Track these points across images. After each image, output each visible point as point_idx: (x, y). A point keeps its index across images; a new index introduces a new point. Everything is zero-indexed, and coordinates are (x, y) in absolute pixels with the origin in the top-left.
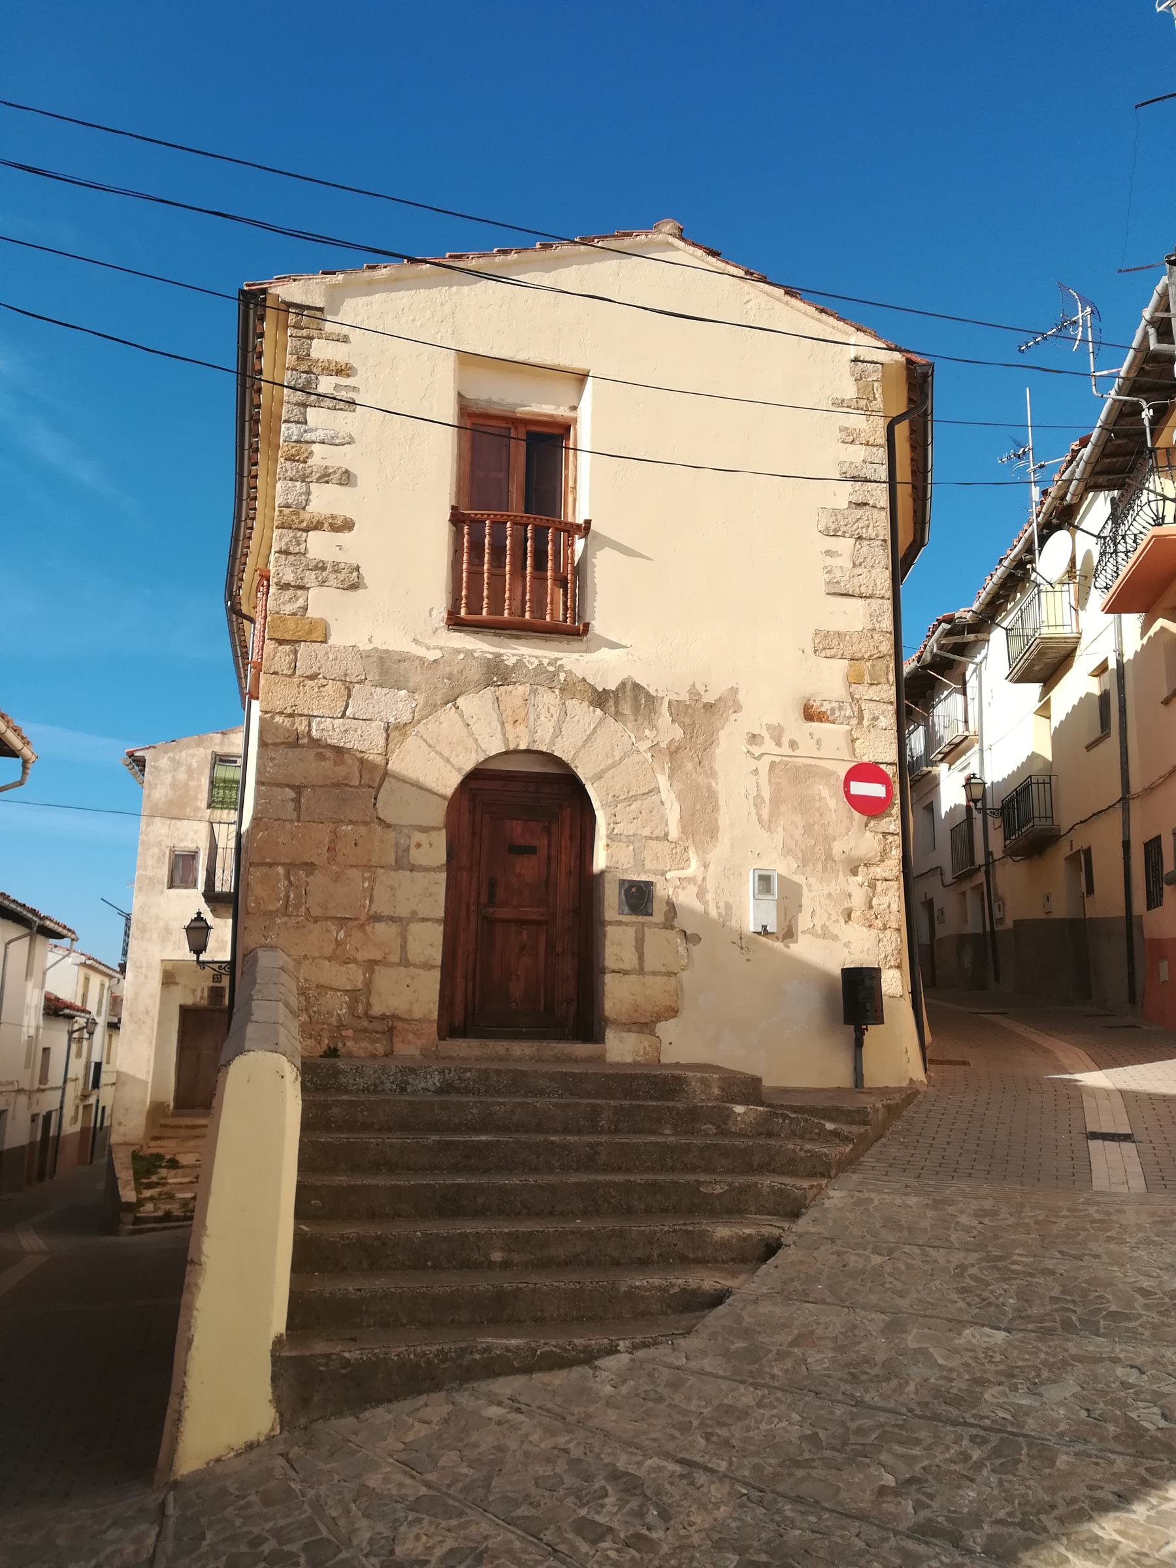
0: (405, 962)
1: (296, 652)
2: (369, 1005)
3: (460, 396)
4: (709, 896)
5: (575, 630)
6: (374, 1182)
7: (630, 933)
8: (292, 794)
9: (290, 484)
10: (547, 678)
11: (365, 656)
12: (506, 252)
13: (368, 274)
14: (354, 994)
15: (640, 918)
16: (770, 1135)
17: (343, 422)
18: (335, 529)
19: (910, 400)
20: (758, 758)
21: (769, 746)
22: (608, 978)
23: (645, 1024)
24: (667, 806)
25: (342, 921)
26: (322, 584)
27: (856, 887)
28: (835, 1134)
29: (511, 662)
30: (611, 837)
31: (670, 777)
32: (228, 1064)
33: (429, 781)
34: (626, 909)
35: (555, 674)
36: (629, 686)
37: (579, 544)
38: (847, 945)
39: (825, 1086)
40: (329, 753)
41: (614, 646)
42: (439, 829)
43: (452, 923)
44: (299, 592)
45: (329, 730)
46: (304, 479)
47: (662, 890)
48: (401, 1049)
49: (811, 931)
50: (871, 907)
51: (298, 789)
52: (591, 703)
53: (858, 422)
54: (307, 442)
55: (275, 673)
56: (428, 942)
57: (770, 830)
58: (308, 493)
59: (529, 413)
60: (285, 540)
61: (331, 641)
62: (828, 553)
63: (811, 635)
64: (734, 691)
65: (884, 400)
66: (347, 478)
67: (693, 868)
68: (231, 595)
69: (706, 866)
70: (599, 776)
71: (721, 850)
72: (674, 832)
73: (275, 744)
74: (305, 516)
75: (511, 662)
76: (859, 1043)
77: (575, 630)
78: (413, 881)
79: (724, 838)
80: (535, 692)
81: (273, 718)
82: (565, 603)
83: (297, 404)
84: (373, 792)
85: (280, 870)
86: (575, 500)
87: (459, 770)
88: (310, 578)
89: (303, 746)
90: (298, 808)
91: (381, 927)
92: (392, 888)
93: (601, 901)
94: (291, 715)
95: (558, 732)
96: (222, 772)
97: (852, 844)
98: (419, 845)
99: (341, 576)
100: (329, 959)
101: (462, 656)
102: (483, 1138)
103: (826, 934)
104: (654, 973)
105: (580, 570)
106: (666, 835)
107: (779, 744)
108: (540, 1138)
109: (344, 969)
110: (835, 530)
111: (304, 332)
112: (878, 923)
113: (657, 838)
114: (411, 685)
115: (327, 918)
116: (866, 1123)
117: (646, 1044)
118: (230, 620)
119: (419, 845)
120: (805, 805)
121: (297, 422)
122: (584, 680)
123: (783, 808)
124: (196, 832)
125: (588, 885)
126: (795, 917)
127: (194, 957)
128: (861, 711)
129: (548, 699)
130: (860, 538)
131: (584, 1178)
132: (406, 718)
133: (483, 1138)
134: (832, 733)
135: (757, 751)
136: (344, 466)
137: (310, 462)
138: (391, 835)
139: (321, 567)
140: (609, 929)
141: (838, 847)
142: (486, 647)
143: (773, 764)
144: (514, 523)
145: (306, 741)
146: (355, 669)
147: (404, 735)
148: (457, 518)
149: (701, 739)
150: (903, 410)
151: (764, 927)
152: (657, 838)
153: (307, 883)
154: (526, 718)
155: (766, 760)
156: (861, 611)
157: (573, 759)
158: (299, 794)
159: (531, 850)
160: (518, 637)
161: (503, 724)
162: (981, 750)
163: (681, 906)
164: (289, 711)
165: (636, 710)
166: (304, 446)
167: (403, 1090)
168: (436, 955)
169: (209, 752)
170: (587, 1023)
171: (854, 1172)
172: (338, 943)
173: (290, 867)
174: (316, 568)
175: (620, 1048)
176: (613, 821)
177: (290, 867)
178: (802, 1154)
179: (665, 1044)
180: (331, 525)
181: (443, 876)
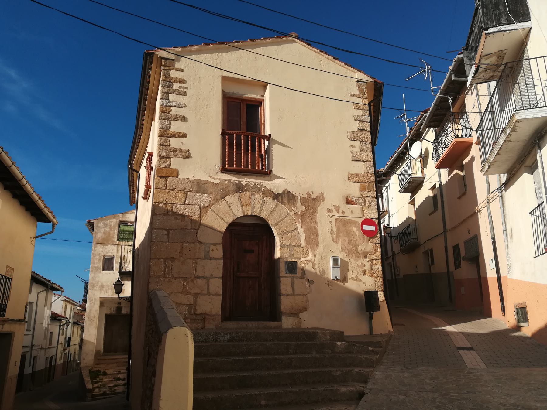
0: (208, 293)
1: (166, 181)
2: (196, 310)
3: (223, 91)
4: (317, 267)
5: (266, 173)
6: (213, 376)
7: (289, 280)
8: (166, 232)
9: (164, 121)
10: (257, 189)
11: (192, 182)
12: (238, 42)
13: (190, 48)
14: (190, 306)
15: (293, 275)
16: (350, 352)
17: (182, 100)
18: (180, 137)
19: (375, 95)
20: (331, 217)
21: (335, 213)
22: (282, 297)
23: (295, 313)
24: (301, 234)
25: (185, 279)
26: (176, 156)
27: (366, 262)
28: (372, 351)
29: (244, 184)
30: (282, 246)
31: (301, 224)
32: (166, 332)
33: (216, 227)
34: (288, 272)
35: (260, 188)
36: (286, 192)
37: (267, 143)
38: (365, 283)
39: (359, 334)
40: (179, 217)
41: (280, 178)
42: (220, 244)
43: (225, 278)
44: (168, 159)
45: (179, 208)
46: (169, 119)
47: (301, 265)
48: (208, 326)
49: (352, 278)
50: (372, 269)
51: (168, 230)
52: (273, 198)
53: (359, 101)
54: (169, 106)
55: (159, 188)
56: (217, 285)
57: (336, 242)
58: (170, 124)
59: (247, 97)
60: (162, 141)
61: (179, 177)
62: (352, 146)
63: (347, 174)
64: (322, 194)
65: (368, 95)
66: (184, 119)
67: (311, 257)
68: (130, 163)
69: (315, 256)
70: (276, 224)
71: (320, 250)
72: (303, 244)
73: (160, 214)
74: (169, 132)
75: (244, 184)
76: (371, 318)
77: (266, 173)
78: (211, 263)
79: (321, 245)
80: (253, 194)
81: (158, 205)
82: (262, 163)
83: (165, 93)
84: (196, 231)
85: (162, 260)
86: (264, 127)
87: (227, 223)
88: (171, 154)
89: (170, 215)
90: (168, 237)
91: (199, 281)
92: (203, 266)
93: (278, 269)
94: (165, 204)
95: (262, 209)
96: (122, 228)
97: (365, 247)
98: (213, 250)
99: (183, 154)
100: (181, 293)
101: (227, 182)
102: (250, 358)
103: (357, 279)
104: (298, 295)
105: (268, 151)
106: (301, 245)
107: (338, 212)
108: (271, 357)
109: (186, 296)
110: (354, 139)
111: (168, 68)
112: (375, 275)
113: (298, 246)
114: (209, 192)
115: (179, 278)
116: (381, 347)
117: (296, 321)
118: (129, 172)
119: (213, 250)
120: (348, 234)
121: (166, 99)
122: (270, 190)
123: (341, 235)
124: (113, 250)
125: (274, 263)
126: (346, 273)
127: (116, 295)
128: (365, 201)
129: (258, 197)
130: (362, 141)
131: (290, 371)
132: (207, 204)
133: (250, 358)
134: (356, 208)
135: (331, 215)
136: (183, 115)
137: (171, 113)
138: (203, 246)
139: (175, 150)
140: (282, 279)
141: (360, 248)
142: (235, 179)
143: (336, 219)
144: (244, 135)
145: (171, 213)
146: (188, 187)
147: (207, 210)
148: (223, 134)
149: (312, 210)
150: (372, 99)
151: (336, 277)
152: (298, 246)
153: (172, 265)
154: (250, 204)
155: (334, 218)
156: (364, 166)
157: (267, 218)
158: (169, 232)
159: (252, 251)
160: (246, 175)
161: (242, 206)
162: (389, 216)
163: (307, 270)
164: (164, 202)
165: (289, 201)
166: (168, 108)
167: (216, 341)
168: (220, 291)
169: (118, 220)
170: (274, 313)
171: (381, 365)
172: (184, 287)
173: (166, 259)
174: (173, 151)
175: (287, 323)
176: (282, 240)
177: (166, 259)
178: (364, 359)
179: (303, 321)
180: (179, 135)
181: (222, 261)
